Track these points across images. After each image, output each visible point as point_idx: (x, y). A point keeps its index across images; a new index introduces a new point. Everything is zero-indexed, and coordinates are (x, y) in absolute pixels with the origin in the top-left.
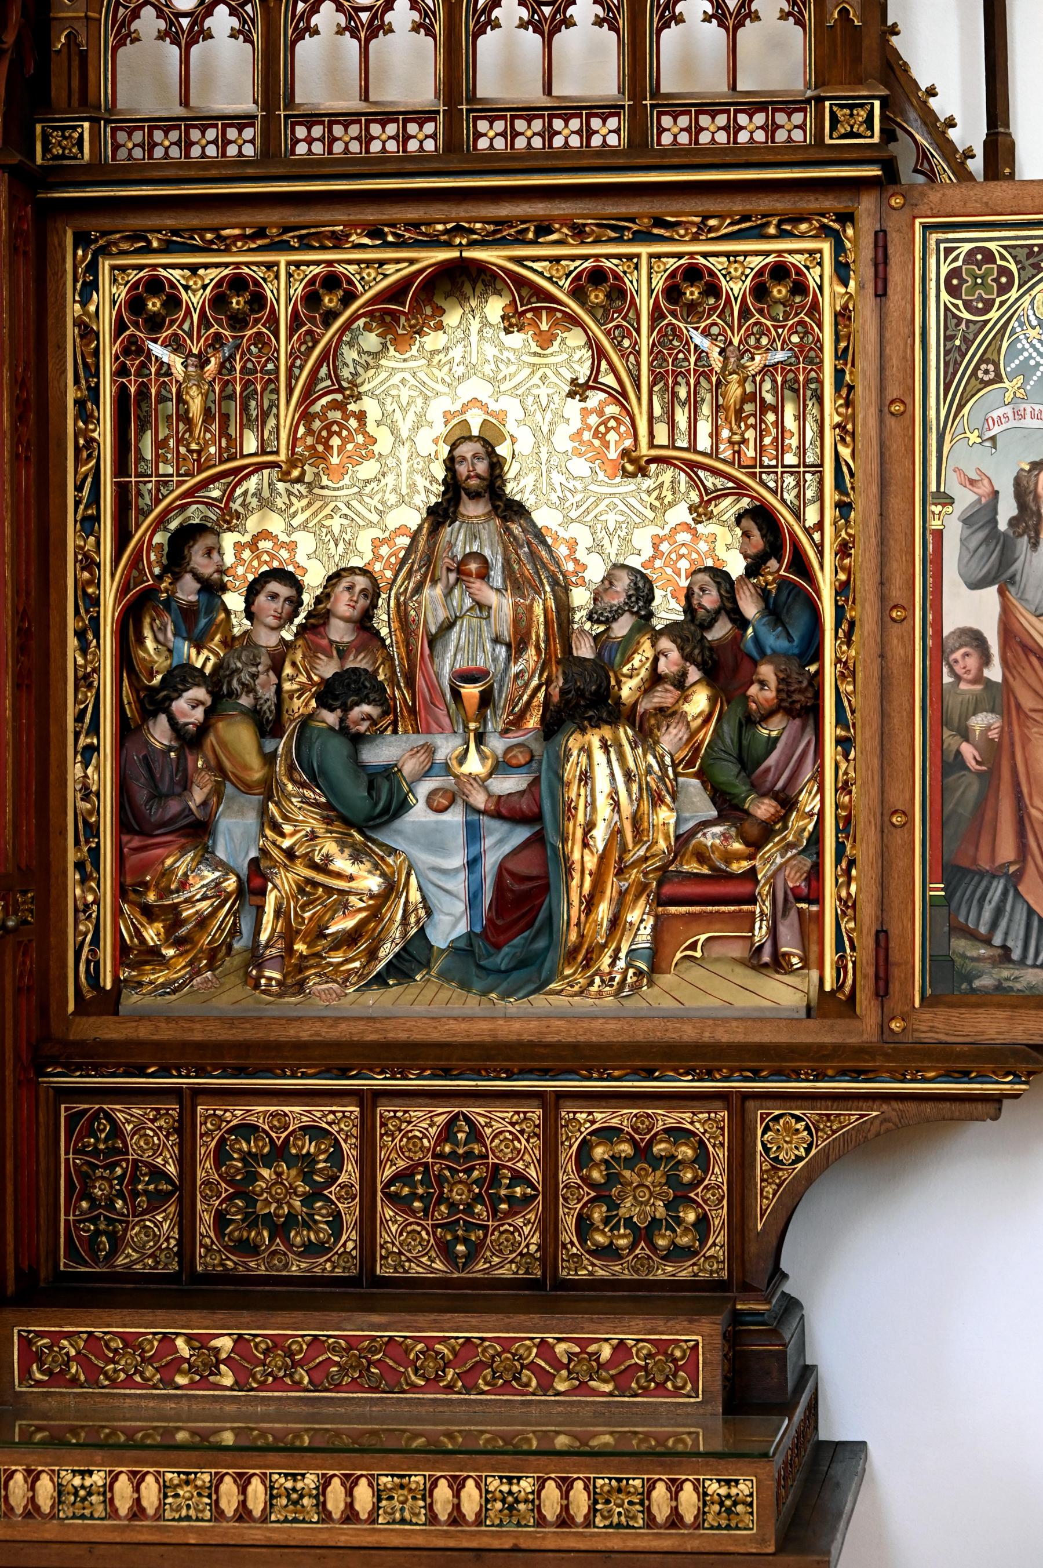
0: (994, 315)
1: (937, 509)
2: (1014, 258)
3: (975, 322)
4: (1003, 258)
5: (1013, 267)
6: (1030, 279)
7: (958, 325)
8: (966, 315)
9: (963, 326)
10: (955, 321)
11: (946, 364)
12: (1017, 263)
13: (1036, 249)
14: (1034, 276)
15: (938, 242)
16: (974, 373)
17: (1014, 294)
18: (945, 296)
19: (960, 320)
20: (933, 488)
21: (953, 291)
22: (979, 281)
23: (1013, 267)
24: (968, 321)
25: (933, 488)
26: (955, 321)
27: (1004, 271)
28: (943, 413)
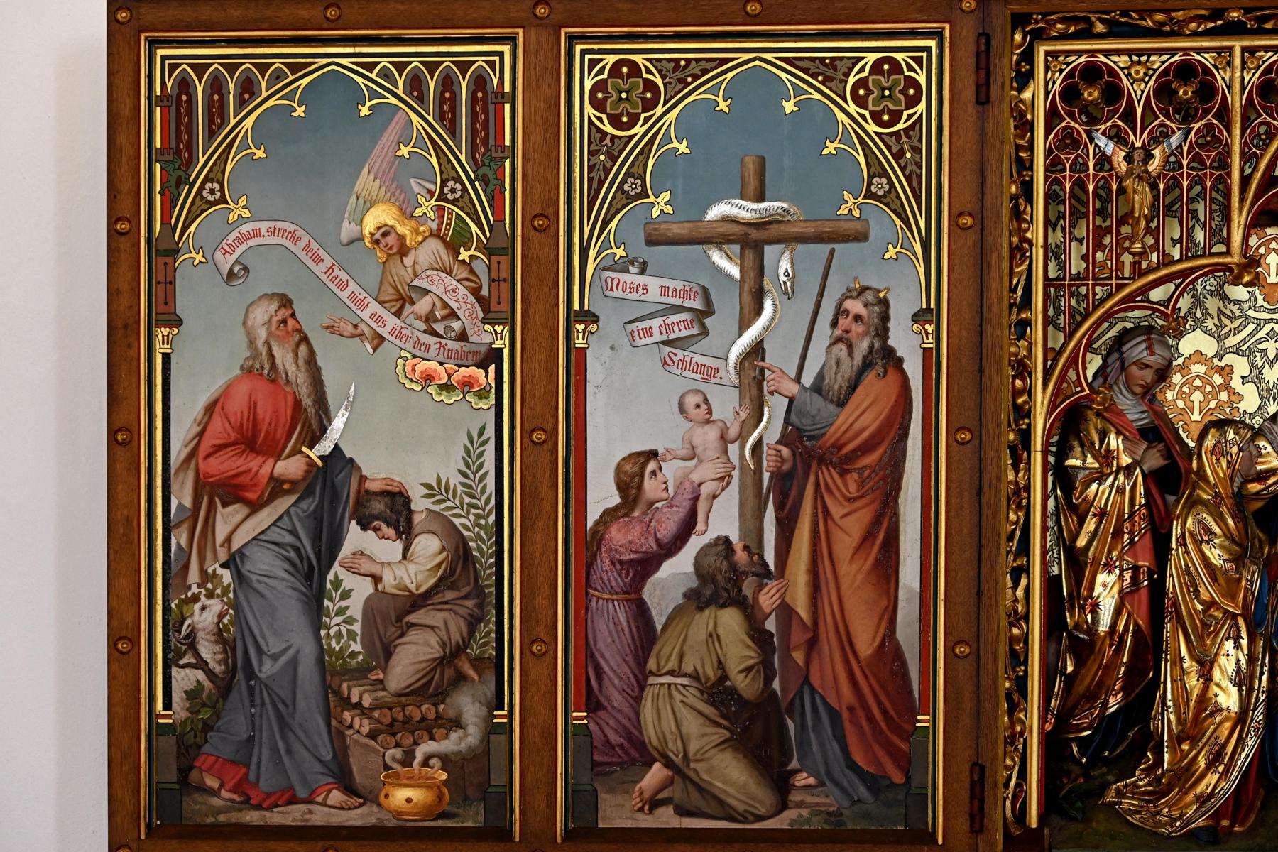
0: (638, 130)
1: (581, 327)
2: (660, 72)
3: (620, 137)
4: (648, 71)
5: (659, 81)
6: (677, 93)
7: (602, 140)
8: (609, 129)
9: (607, 141)
10: (599, 135)
11: (590, 180)
12: (663, 77)
13: (683, 63)
14: (681, 91)
15: (583, 52)
16: (620, 187)
17: (659, 110)
18: (589, 110)
19: (605, 134)
20: (576, 306)
21: (599, 106)
22: (624, 95)
23: (659, 81)
24: (613, 137)
25: (576, 306)
26: (599, 135)
27: (650, 85)
28: (587, 230)
